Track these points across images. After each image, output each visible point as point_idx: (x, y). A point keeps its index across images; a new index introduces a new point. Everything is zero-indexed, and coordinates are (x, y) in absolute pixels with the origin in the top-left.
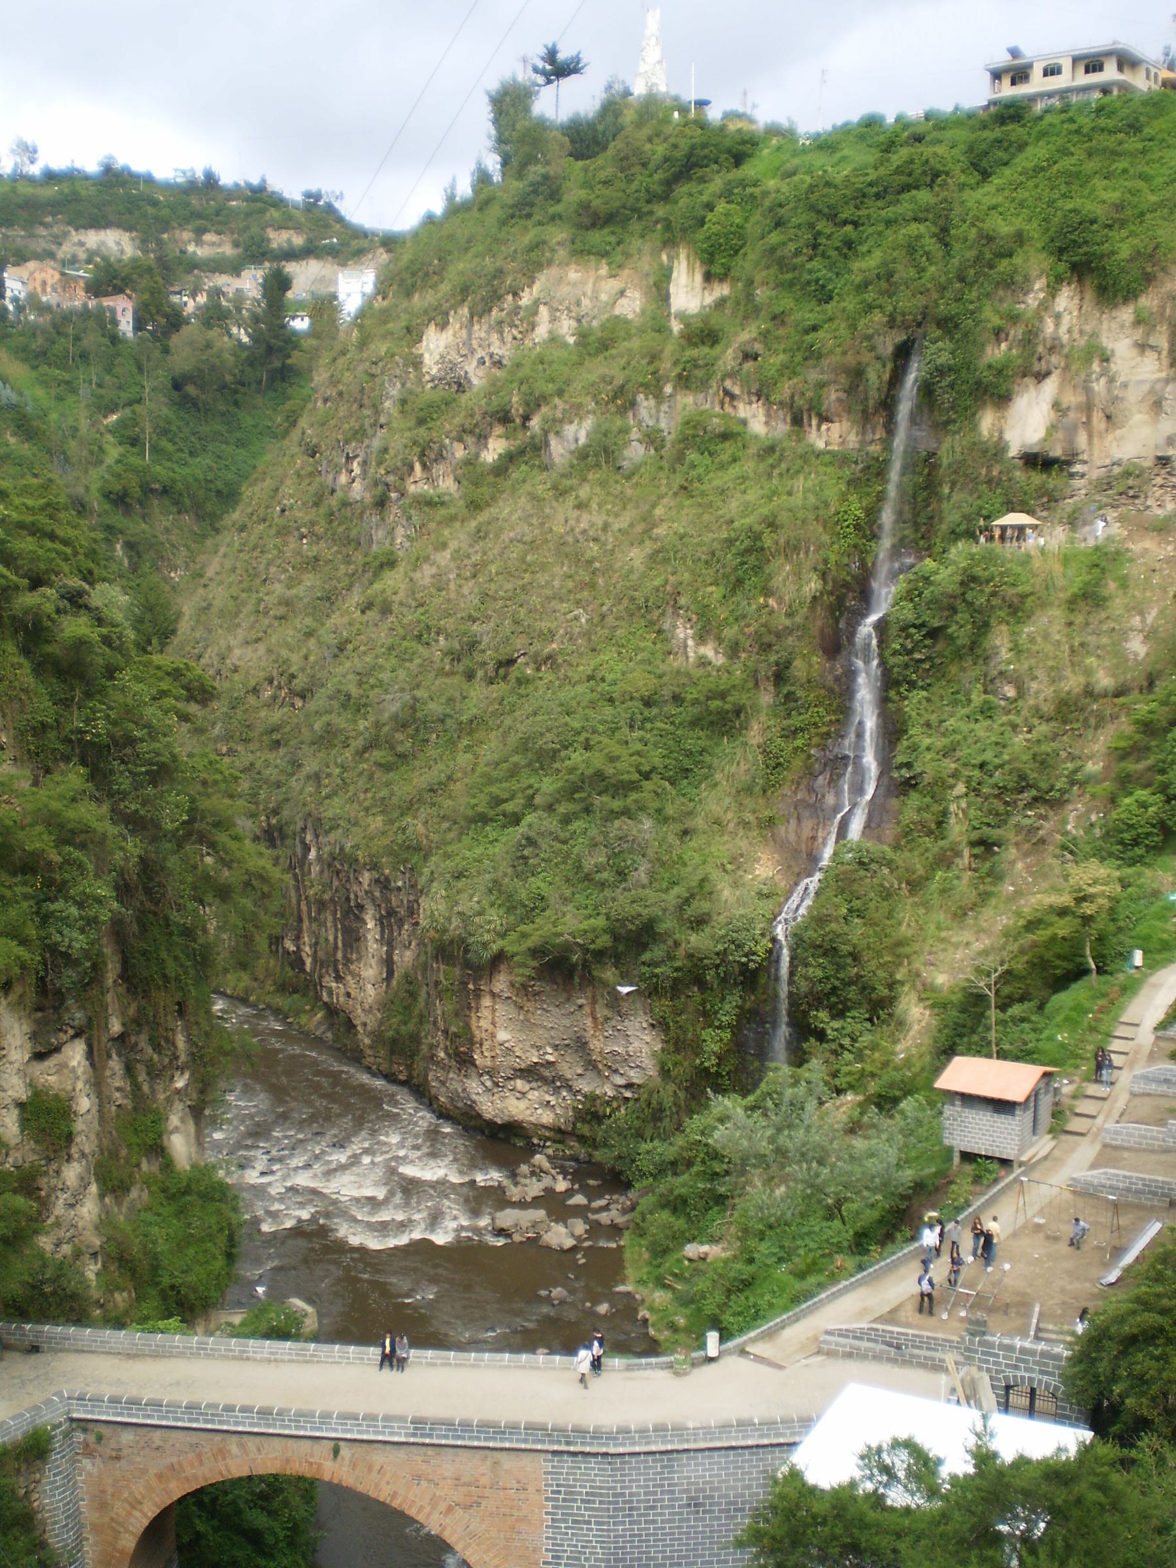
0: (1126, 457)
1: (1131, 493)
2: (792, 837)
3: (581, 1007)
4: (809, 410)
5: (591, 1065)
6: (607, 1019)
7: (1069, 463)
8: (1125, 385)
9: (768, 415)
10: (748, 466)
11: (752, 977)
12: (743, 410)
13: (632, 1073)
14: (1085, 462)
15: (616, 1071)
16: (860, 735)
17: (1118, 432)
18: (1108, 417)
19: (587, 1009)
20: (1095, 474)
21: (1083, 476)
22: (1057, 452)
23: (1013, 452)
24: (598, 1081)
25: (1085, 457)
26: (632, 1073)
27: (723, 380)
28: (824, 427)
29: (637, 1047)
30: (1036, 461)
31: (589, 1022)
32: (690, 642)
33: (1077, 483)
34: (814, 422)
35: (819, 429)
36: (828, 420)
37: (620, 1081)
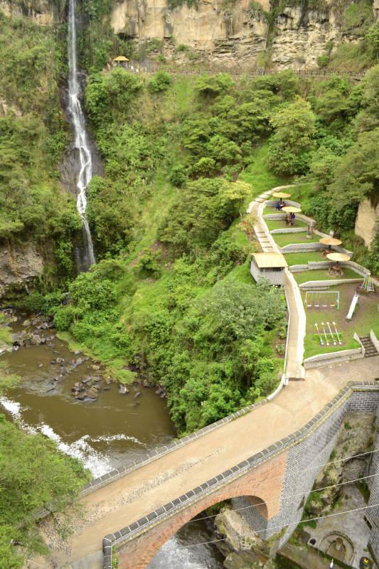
0: (151, 37)
1: (156, 50)
2: (69, 180)
3: (6, 254)
4: (31, 8)
5: (12, 274)
6: (18, 256)
9: (11, 8)
10: (10, 31)
11: (75, 234)
13: (30, 273)
14: (138, 38)
15: (23, 274)
16: (81, 139)
17: (147, 27)
18: (143, 21)
19: (9, 254)
23: (116, 32)
24: (14, 279)
26: (30, 273)
29: (34, 264)
30: (123, 36)
31: (10, 259)
32: (5, 106)
34: (34, 13)
35: (35, 15)
36: (39, 12)
37: (24, 276)
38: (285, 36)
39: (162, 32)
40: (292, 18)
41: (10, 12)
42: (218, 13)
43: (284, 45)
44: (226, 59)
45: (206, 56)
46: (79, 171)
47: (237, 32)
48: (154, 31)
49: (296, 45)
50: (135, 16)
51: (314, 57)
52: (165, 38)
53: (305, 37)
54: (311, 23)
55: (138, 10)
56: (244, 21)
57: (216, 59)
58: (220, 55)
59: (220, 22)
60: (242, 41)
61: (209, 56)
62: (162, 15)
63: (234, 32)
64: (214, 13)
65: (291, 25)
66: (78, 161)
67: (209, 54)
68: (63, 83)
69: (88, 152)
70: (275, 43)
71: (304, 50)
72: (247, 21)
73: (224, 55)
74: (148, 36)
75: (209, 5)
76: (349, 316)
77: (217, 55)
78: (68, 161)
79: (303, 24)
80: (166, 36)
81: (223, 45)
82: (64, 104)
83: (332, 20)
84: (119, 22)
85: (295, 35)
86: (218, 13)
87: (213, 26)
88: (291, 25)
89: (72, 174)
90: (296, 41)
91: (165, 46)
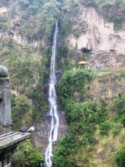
0: (103, 50)
1: (105, 57)
2: (42, 136)
7: (91, 51)
8: (102, 34)
9: (22, 38)
12: (15, 38)
14: (94, 51)
16: (53, 111)
17: (100, 45)
18: (98, 42)
20: (96, 53)
21: (94, 54)
22: (89, 48)
25: (94, 50)
27: (10, 30)
28: (36, 42)
30: (85, 50)
33: (92, 55)
34: (34, 40)
35: (35, 42)
39: (109, 47)
41: (21, 40)
46: (50, 130)
48: (105, 47)
50: (93, 39)
52: (111, 50)
55: (95, 36)
62: (109, 38)
66: (50, 123)
68: (46, 78)
69: (57, 119)
74: (100, 50)
78: (44, 124)
80: (112, 49)
82: (46, 91)
84: (82, 42)
89: (46, 132)
91: (111, 55)
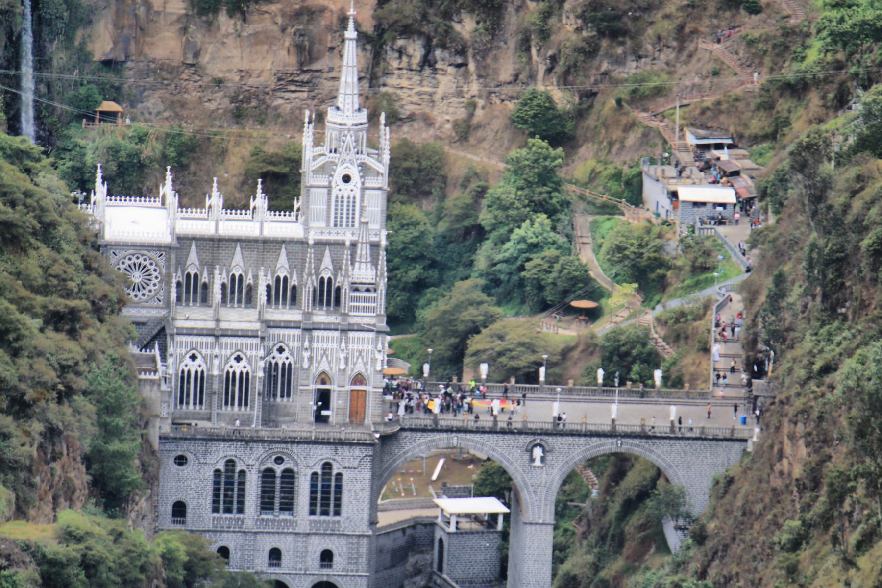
0: (158, 57)
38: (400, 77)
40: (410, 57)
42: (283, 30)
43: (399, 91)
44: (298, 103)
45: (261, 97)
47: (317, 59)
49: (419, 93)
51: (447, 117)
52: (184, 63)
53: (434, 82)
54: (438, 66)
56: (329, 45)
57: (280, 101)
58: (287, 95)
59: (287, 44)
60: (325, 75)
61: (267, 97)
63: (312, 59)
64: (275, 28)
65: (409, 64)
67: (267, 93)
70: (384, 85)
71: (433, 102)
72: (334, 44)
73: (294, 95)
75: (267, 15)
76: (434, 477)
77: (283, 94)
79: (427, 62)
81: (292, 81)
83: (472, 66)
85: (417, 78)
86: (283, 30)
87: (274, 48)
88: (409, 64)
90: (418, 89)
91: (184, 76)
